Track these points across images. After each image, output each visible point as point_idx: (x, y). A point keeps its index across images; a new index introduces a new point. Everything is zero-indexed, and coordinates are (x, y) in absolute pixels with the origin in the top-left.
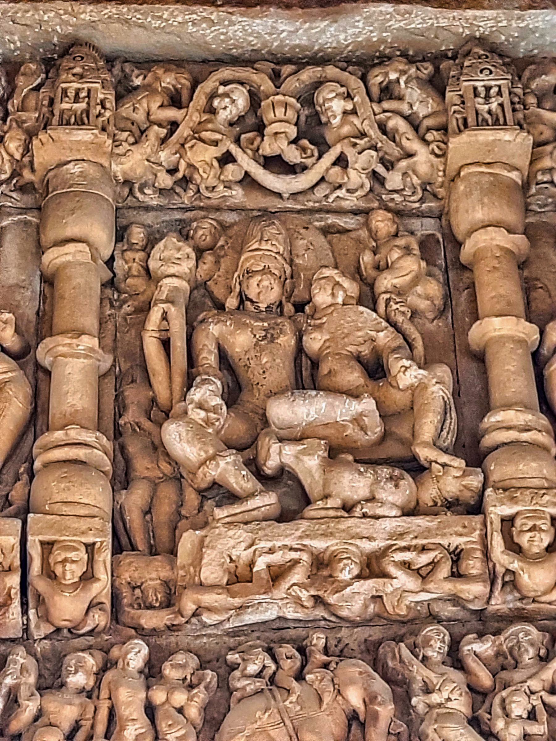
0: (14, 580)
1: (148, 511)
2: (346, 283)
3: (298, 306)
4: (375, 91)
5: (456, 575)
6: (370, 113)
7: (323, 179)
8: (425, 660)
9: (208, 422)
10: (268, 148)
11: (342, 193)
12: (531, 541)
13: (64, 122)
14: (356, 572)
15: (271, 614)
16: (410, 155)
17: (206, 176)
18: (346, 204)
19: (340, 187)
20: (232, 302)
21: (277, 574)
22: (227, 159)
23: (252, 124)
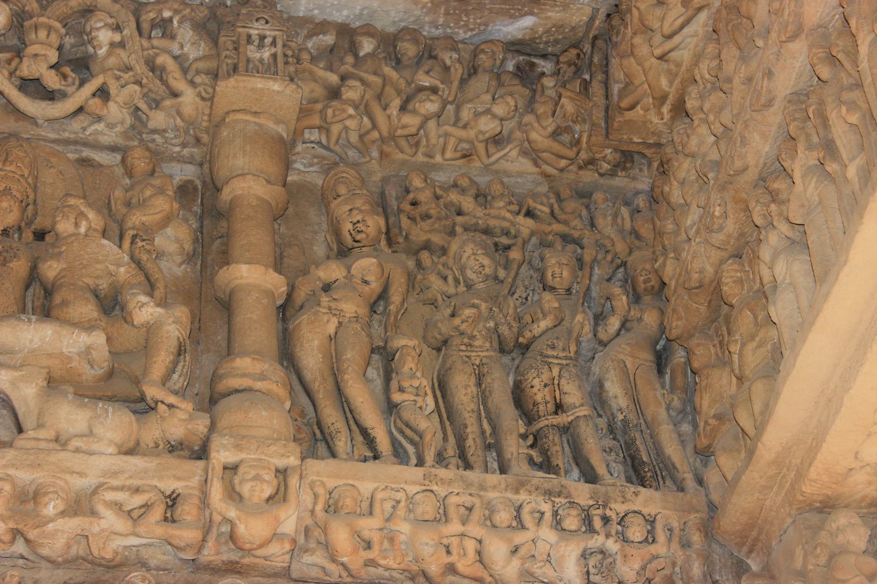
2: (91, 215)
4: (146, 26)
5: (169, 519)
6: (137, 47)
7: (80, 110)
10: (28, 69)
11: (100, 127)
12: (252, 490)
14: (61, 507)
19: (99, 119)
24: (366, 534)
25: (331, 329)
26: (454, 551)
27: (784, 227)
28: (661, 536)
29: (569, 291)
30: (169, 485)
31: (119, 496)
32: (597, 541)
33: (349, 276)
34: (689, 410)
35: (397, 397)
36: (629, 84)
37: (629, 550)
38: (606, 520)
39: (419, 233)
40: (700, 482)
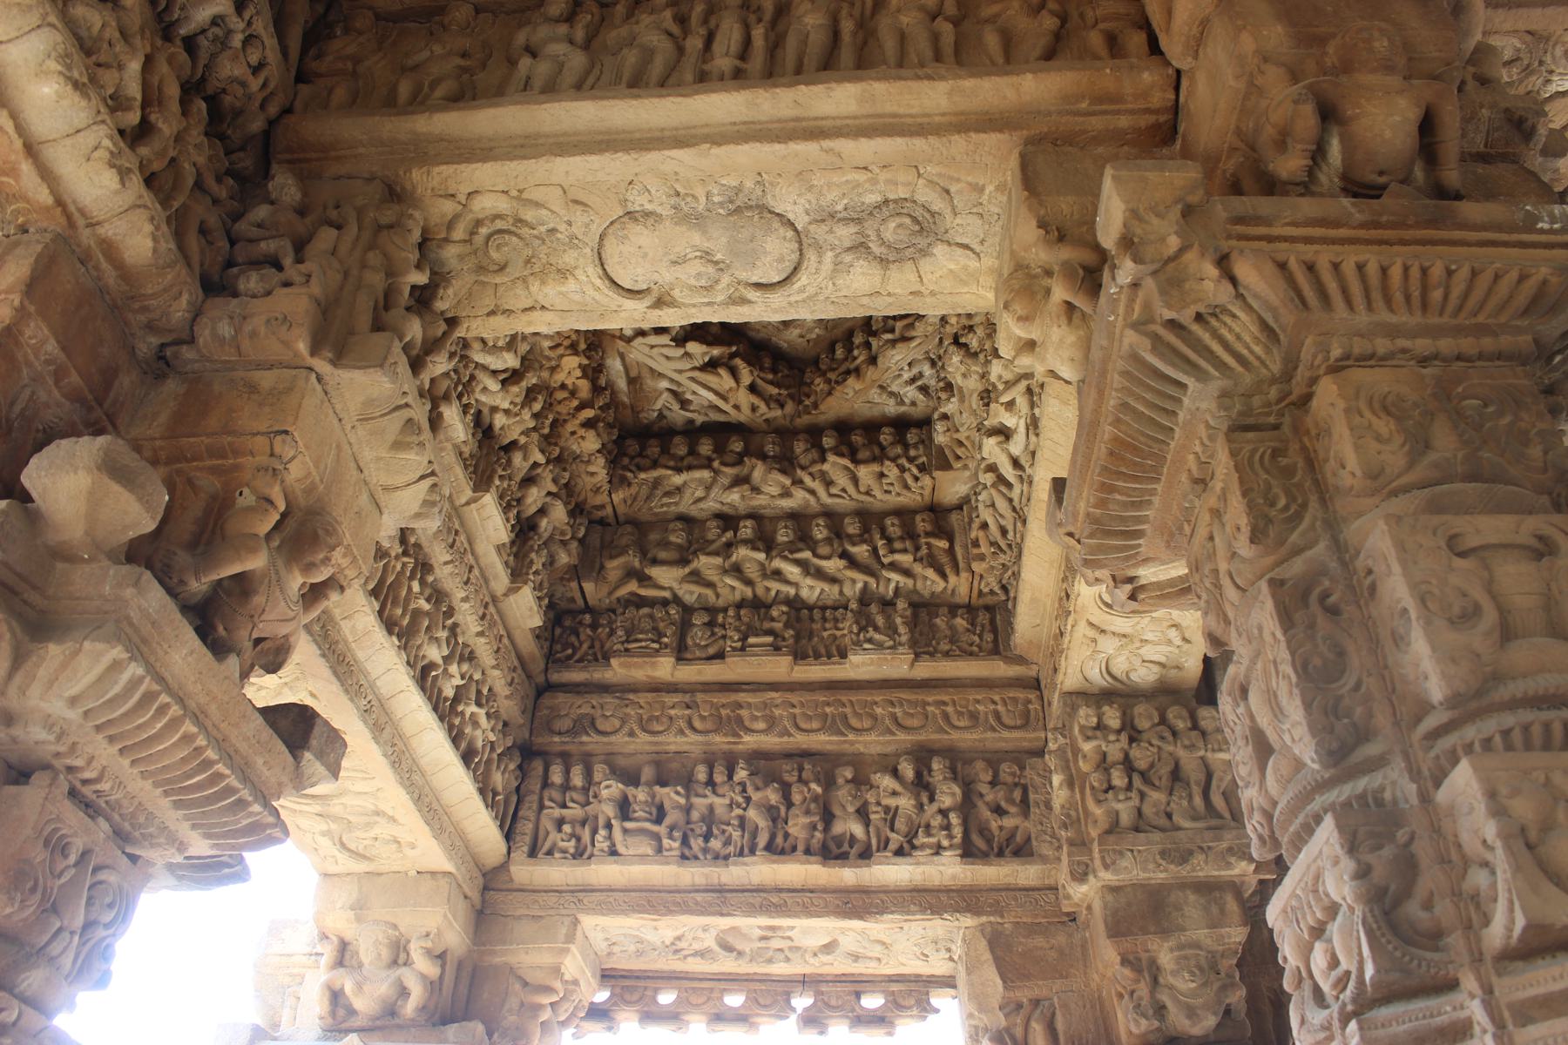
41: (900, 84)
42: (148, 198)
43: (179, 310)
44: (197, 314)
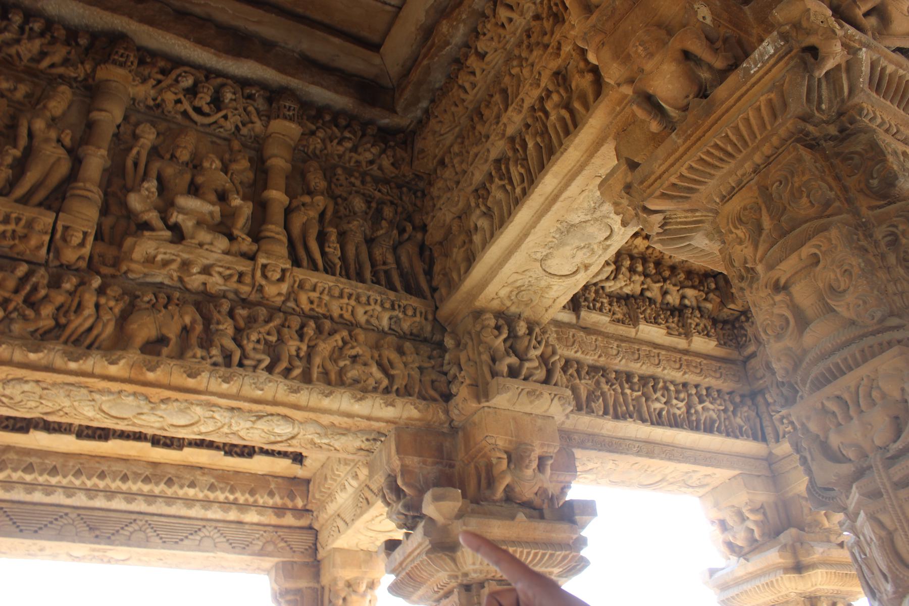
0: (47, 238)
1: (112, 228)
3: (195, 165)
5: (239, 281)
7: (215, 122)
8: (219, 312)
9: (148, 197)
10: (197, 103)
11: (222, 130)
13: (114, 62)
14: (199, 270)
15: (159, 279)
16: (253, 123)
17: (169, 106)
18: (222, 135)
19: (221, 127)
20: (168, 156)
21: (166, 263)
22: (179, 101)
23: (192, 92)
24: (312, 298)
25: (304, 220)
26: (344, 309)
27: (483, 208)
28: (418, 314)
29: (391, 221)
30: (241, 269)
31: (221, 270)
32: (396, 313)
33: (312, 202)
34: (429, 273)
35: (327, 250)
36: (423, 151)
37: (406, 318)
38: (399, 306)
39: (338, 192)
40: (433, 297)
41: (559, 162)
42: (405, 400)
43: (442, 416)
44: (447, 412)
